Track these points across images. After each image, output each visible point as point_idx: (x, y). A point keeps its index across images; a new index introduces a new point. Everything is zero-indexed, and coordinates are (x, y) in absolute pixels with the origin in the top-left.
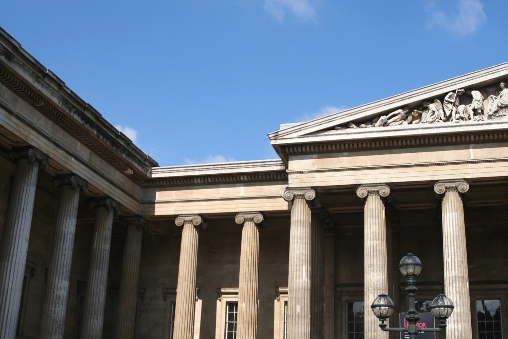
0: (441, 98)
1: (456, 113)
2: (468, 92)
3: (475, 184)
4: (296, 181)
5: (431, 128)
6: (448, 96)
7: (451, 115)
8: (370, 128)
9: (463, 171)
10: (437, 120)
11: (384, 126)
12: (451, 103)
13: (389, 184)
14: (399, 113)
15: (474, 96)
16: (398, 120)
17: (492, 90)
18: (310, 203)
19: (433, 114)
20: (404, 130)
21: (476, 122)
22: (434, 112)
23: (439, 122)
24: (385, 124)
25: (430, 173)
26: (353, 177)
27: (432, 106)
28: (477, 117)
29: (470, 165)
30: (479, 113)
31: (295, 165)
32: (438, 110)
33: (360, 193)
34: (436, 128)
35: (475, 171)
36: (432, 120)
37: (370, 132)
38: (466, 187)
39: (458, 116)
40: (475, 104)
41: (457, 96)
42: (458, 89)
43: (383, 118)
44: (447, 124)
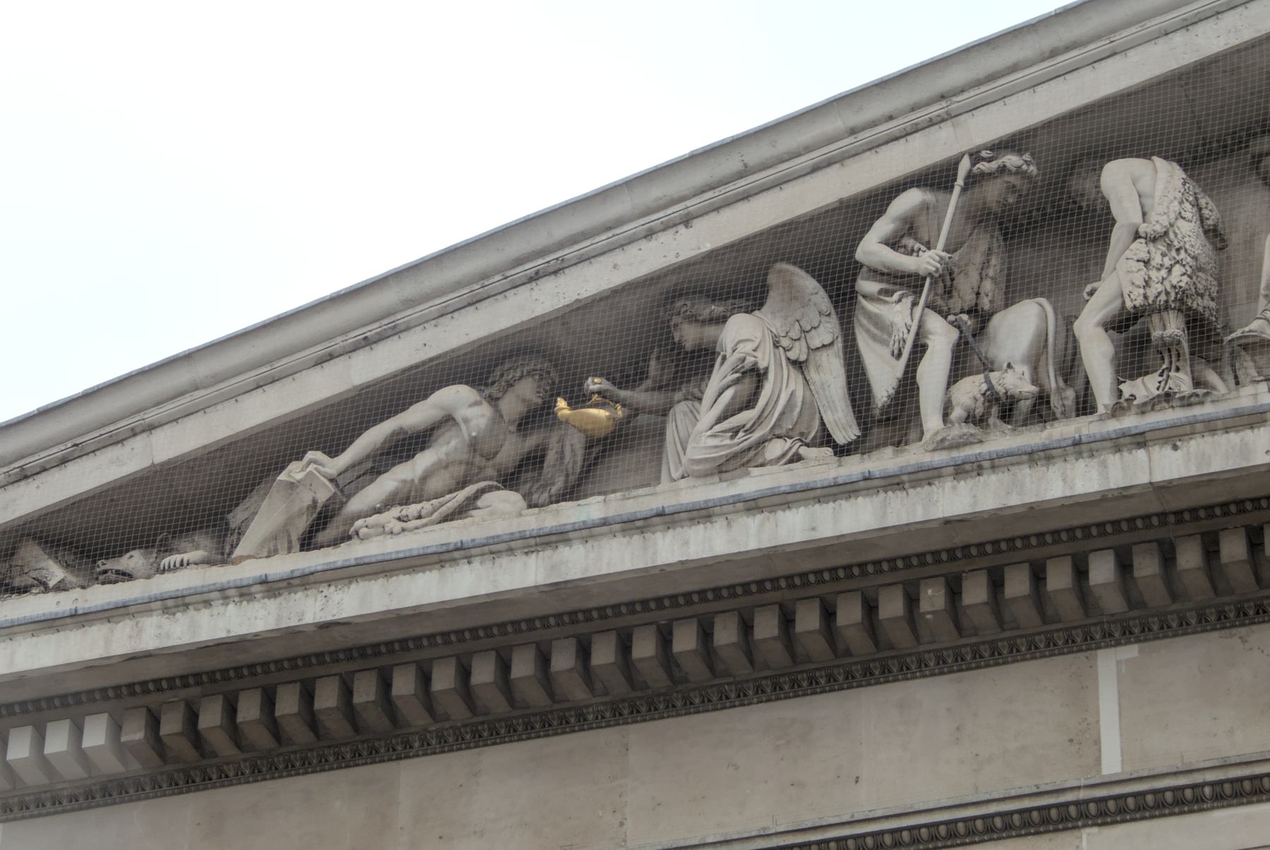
1: (959, 369)
2: (1079, 184)
5: (702, 514)
6: (883, 226)
7: (908, 386)
10: (776, 448)
11: (308, 543)
12: (911, 282)
14: (448, 420)
15: (1125, 212)
16: (435, 484)
19: (749, 404)
22: (756, 375)
23: (797, 458)
28: (1145, 387)
30: (1169, 347)
32: (798, 365)
34: (753, 505)
36: (729, 445)
39: (970, 390)
41: (978, 218)
42: (975, 156)
44: (884, 461)
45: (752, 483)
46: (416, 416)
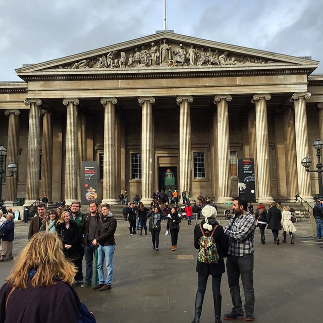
0: (106, 55)
3: (120, 99)
4: (32, 95)
8: (69, 69)
9: (115, 93)
13: (79, 99)
17: (132, 52)
18: (40, 107)
20: (86, 71)
21: (122, 69)
24: (77, 67)
25: (99, 94)
26: (61, 94)
27: (100, 59)
28: (123, 66)
29: (118, 90)
31: (32, 86)
33: (65, 102)
35: (121, 93)
37: (69, 71)
38: (115, 101)
40: (122, 59)
43: (76, 64)
44: (107, 69)
45: (102, 69)
46: (83, 61)
